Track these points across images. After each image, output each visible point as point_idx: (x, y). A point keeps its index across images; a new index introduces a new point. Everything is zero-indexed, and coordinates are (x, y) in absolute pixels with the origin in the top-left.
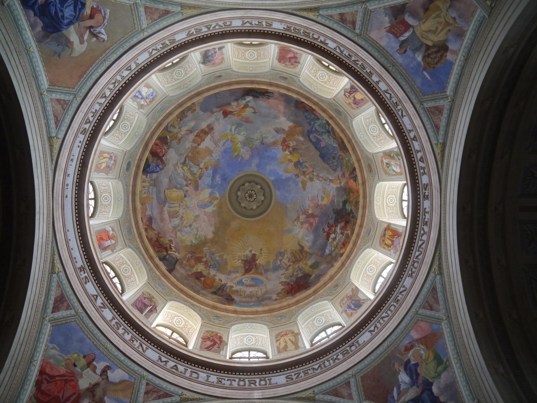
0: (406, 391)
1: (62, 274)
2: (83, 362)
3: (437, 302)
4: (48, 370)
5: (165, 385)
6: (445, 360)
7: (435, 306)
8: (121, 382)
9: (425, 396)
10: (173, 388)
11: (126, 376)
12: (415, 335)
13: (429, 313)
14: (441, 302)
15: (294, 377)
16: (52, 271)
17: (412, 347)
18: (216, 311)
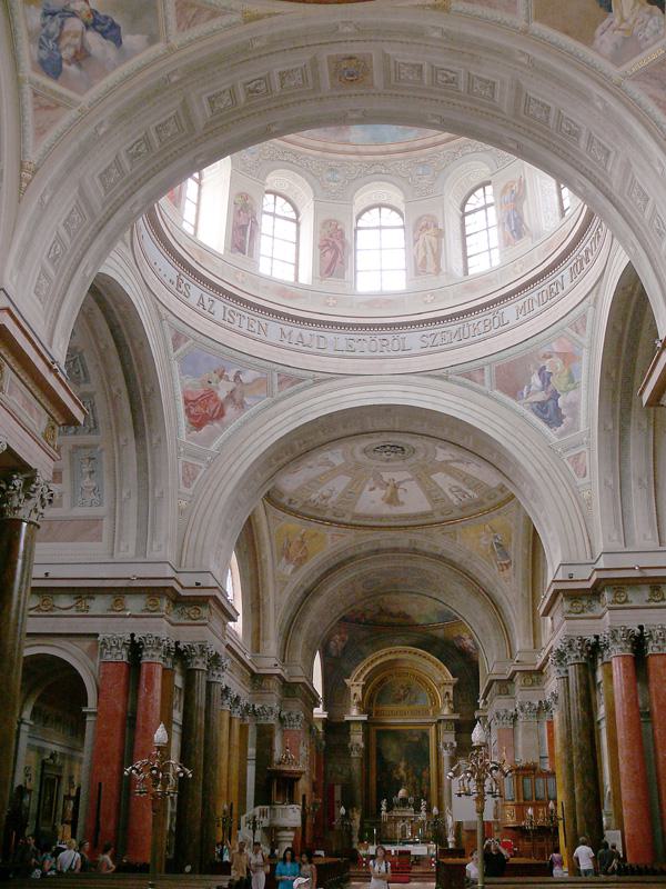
0: (535, 392)
1: (171, 317)
2: (216, 377)
3: (584, 327)
4: (191, 398)
5: (295, 372)
6: (576, 381)
7: (581, 331)
8: (254, 381)
9: (551, 403)
10: (304, 373)
11: (258, 375)
12: (555, 347)
13: (574, 334)
14: (588, 332)
15: (430, 340)
16: (161, 320)
17: (550, 357)
18: (331, 155)
